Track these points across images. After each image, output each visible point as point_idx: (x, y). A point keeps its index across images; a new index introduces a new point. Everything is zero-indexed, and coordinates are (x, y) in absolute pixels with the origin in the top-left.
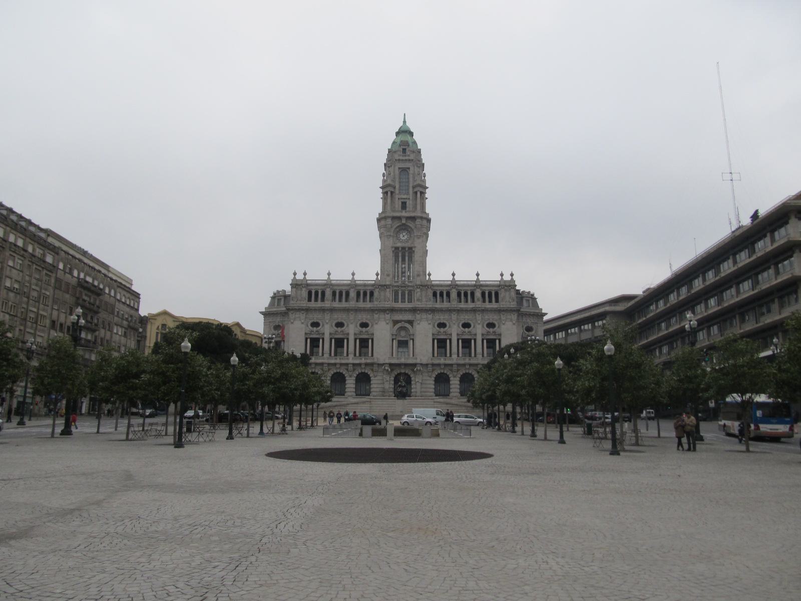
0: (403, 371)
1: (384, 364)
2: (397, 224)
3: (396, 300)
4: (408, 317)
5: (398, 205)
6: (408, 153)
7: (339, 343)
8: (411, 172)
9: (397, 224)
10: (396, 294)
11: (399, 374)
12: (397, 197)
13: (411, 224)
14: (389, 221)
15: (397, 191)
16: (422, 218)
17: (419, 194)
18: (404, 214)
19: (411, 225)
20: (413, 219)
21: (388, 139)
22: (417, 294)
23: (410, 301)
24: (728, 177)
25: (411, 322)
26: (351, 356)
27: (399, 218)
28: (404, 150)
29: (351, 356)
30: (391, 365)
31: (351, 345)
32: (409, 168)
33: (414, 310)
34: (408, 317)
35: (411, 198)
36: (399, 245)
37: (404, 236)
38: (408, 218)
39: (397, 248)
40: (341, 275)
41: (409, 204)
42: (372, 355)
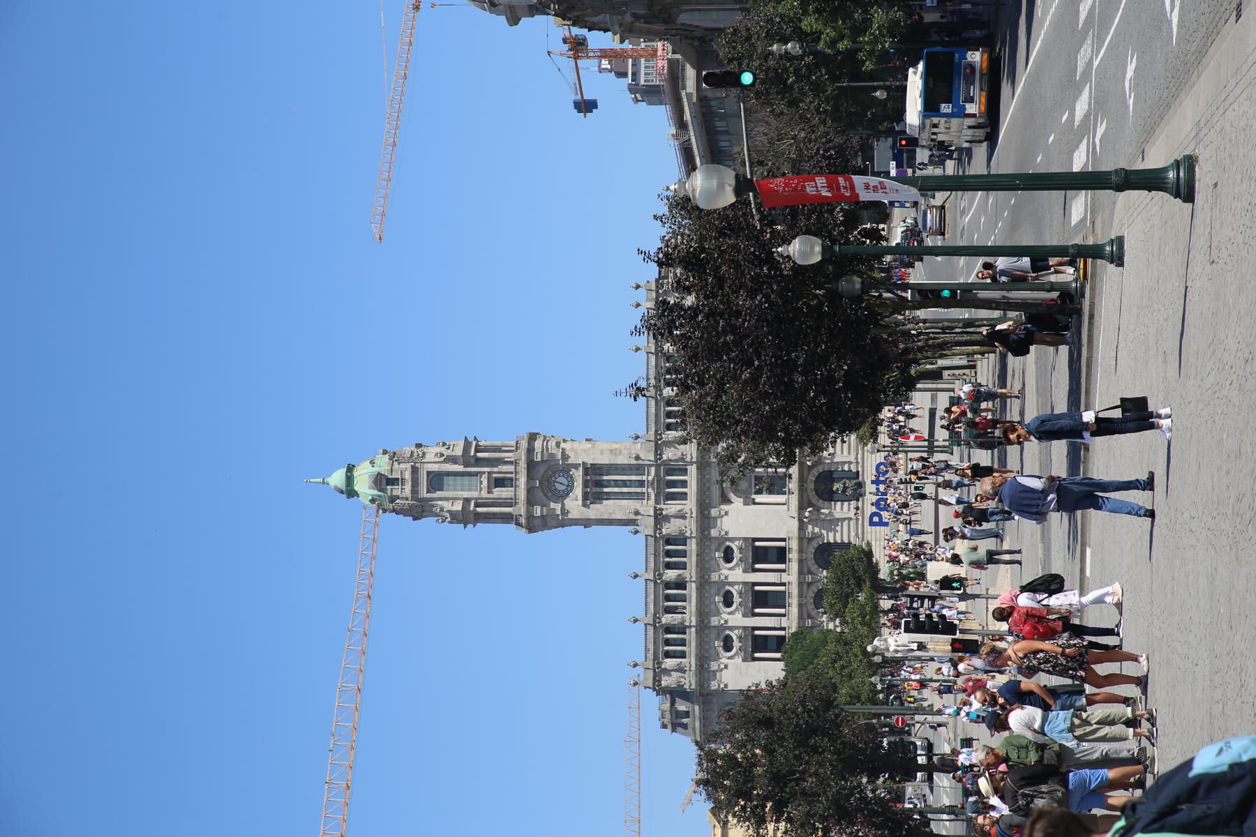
0: (812, 486)
1: (800, 520)
3: (684, 496)
6: (396, 475)
7: (761, 599)
8: (435, 467)
11: (816, 491)
12: (484, 494)
15: (475, 494)
16: (530, 450)
17: (480, 455)
18: (522, 481)
19: (542, 471)
26: (785, 578)
27: (530, 491)
29: (785, 578)
30: (801, 508)
31: (765, 577)
32: (428, 473)
35: (488, 469)
38: (530, 477)
39: (585, 496)
40: (636, 599)
42: (783, 540)
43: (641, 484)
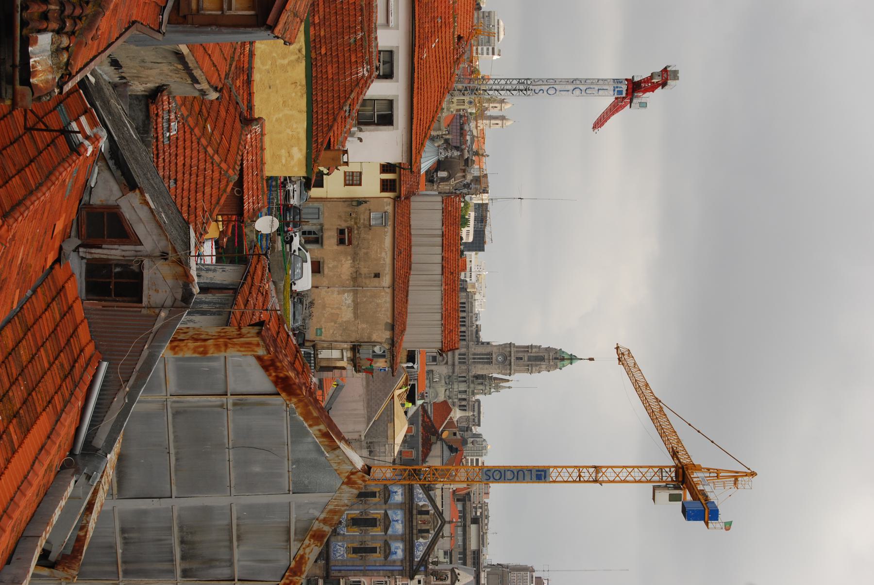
2: (507, 354)
4: (450, 362)
5: (520, 355)
9: (507, 354)
10: (464, 355)
13: (507, 362)
14: (508, 349)
16: (510, 369)
20: (510, 364)
21: (569, 350)
22: (464, 367)
23: (460, 363)
24: (546, 569)
25: (447, 363)
28: (556, 359)
33: (453, 365)
34: (450, 362)
36: (494, 356)
37: (500, 359)
41: (521, 362)
43: (474, 359)
